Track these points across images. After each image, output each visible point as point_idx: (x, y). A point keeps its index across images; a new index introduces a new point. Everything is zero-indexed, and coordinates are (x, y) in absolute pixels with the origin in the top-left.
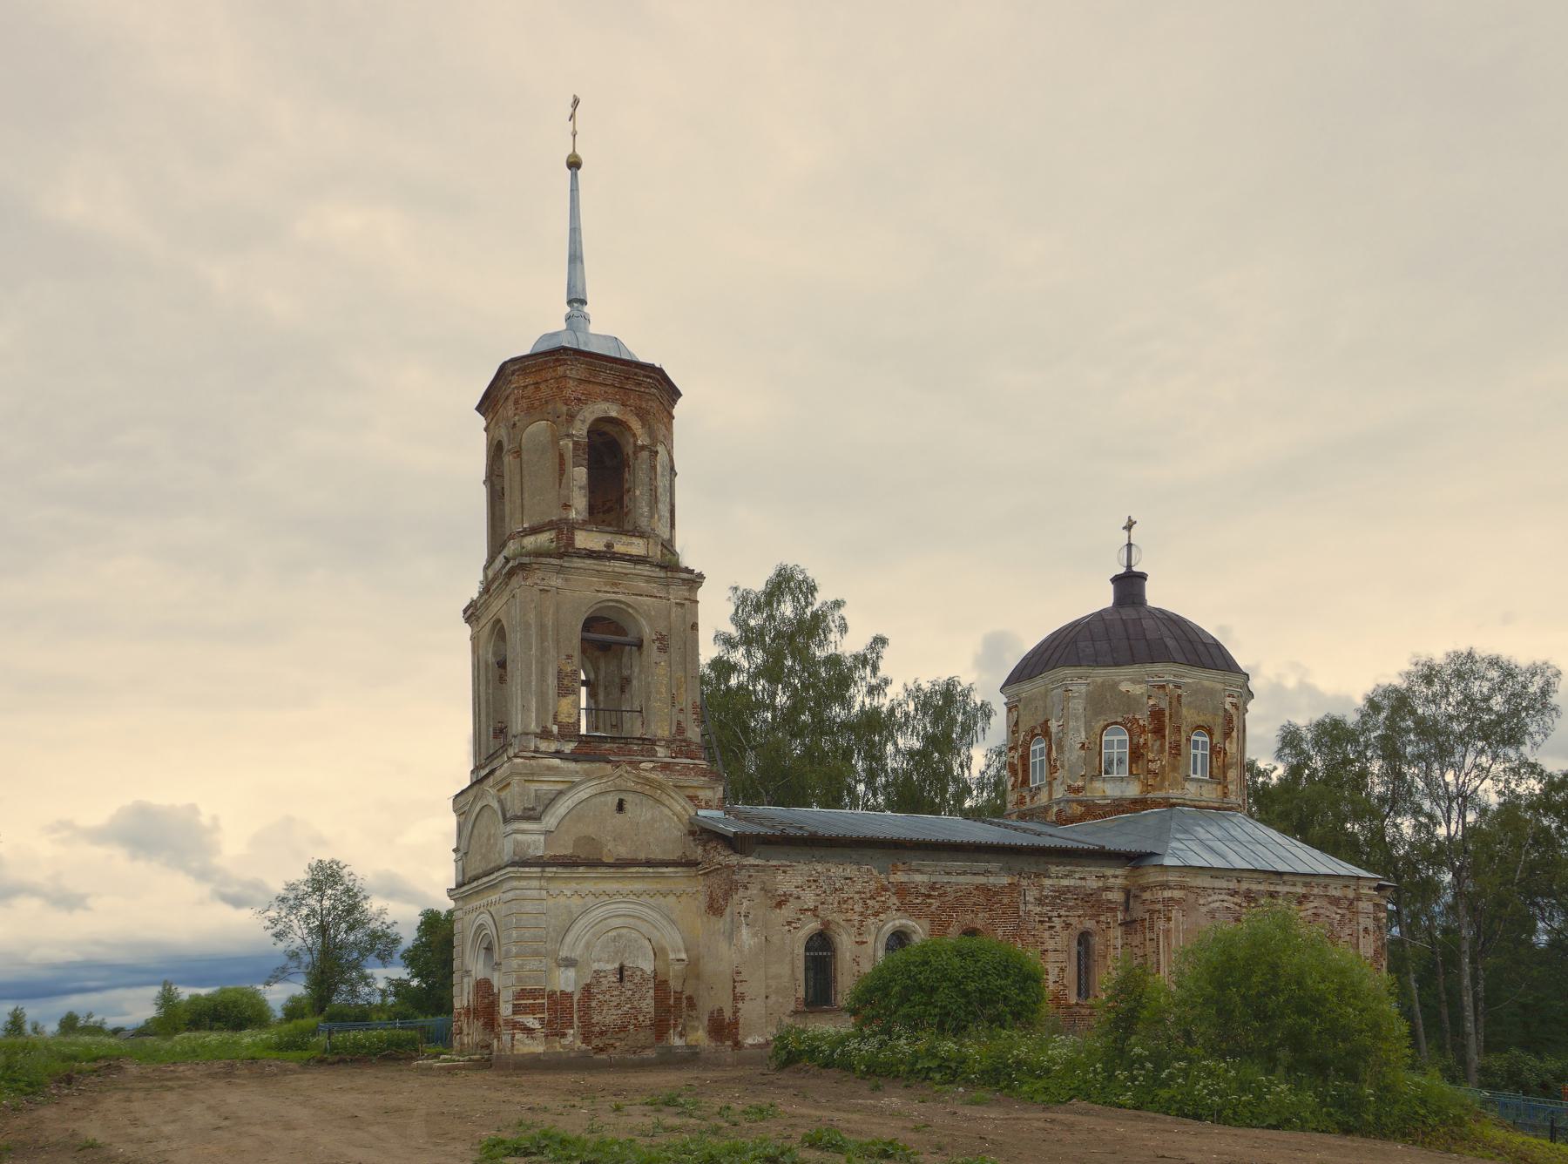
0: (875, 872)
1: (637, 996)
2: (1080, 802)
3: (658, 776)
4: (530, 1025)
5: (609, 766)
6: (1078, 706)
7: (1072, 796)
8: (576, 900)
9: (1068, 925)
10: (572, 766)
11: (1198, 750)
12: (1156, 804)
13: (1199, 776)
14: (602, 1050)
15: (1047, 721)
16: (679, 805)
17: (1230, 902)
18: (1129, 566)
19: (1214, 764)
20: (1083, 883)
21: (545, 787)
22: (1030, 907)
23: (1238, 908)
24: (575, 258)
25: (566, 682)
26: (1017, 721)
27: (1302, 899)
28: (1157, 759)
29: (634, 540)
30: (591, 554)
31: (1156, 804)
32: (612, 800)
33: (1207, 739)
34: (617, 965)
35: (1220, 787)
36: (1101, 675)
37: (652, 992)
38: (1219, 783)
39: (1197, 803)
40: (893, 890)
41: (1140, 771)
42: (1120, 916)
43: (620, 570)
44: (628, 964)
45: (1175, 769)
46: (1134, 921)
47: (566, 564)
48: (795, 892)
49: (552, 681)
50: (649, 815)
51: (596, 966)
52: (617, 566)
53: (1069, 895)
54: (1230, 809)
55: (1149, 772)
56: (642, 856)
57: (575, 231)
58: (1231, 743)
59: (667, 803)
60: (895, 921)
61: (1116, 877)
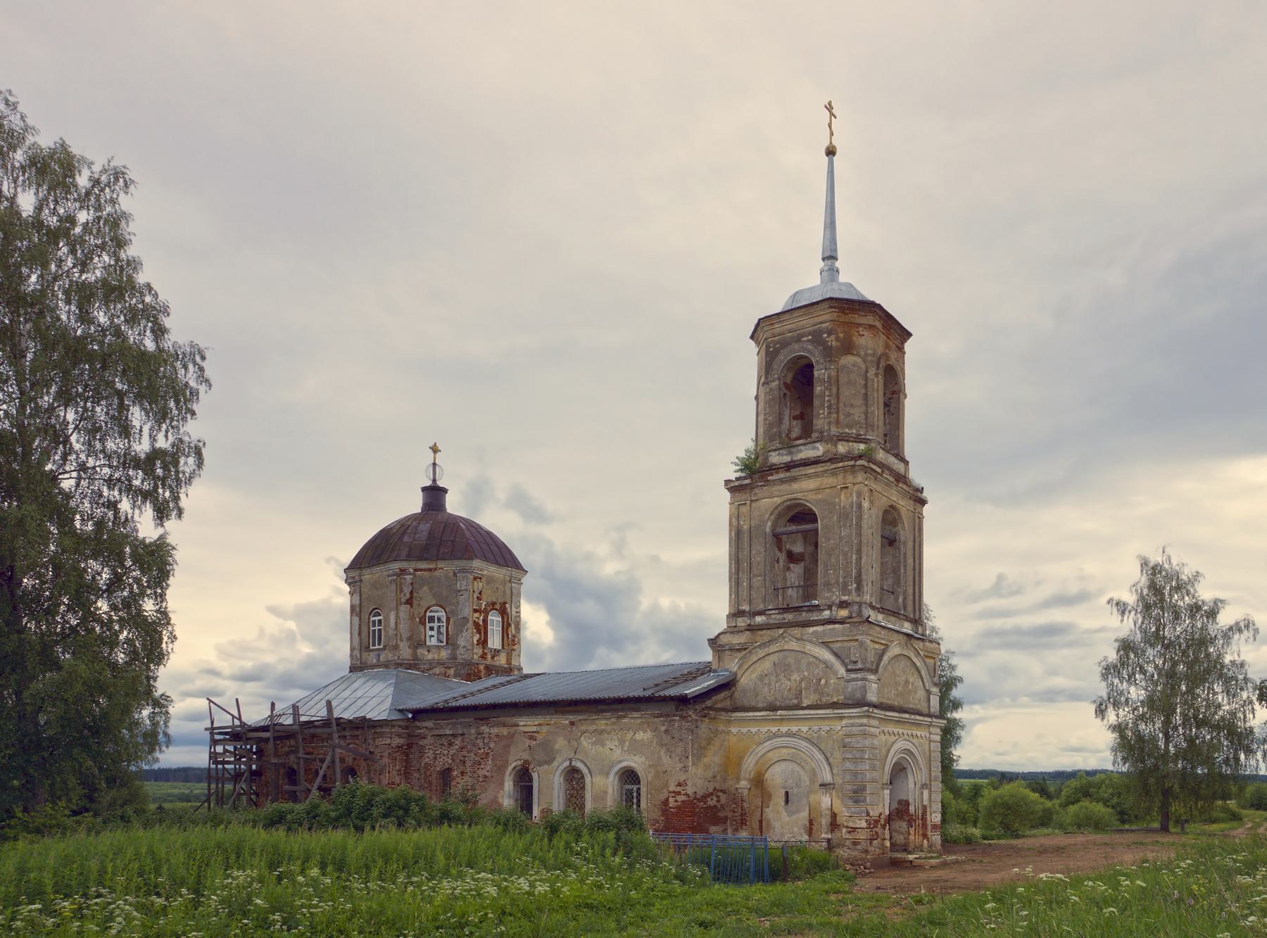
15: (505, 603)
18: (434, 480)
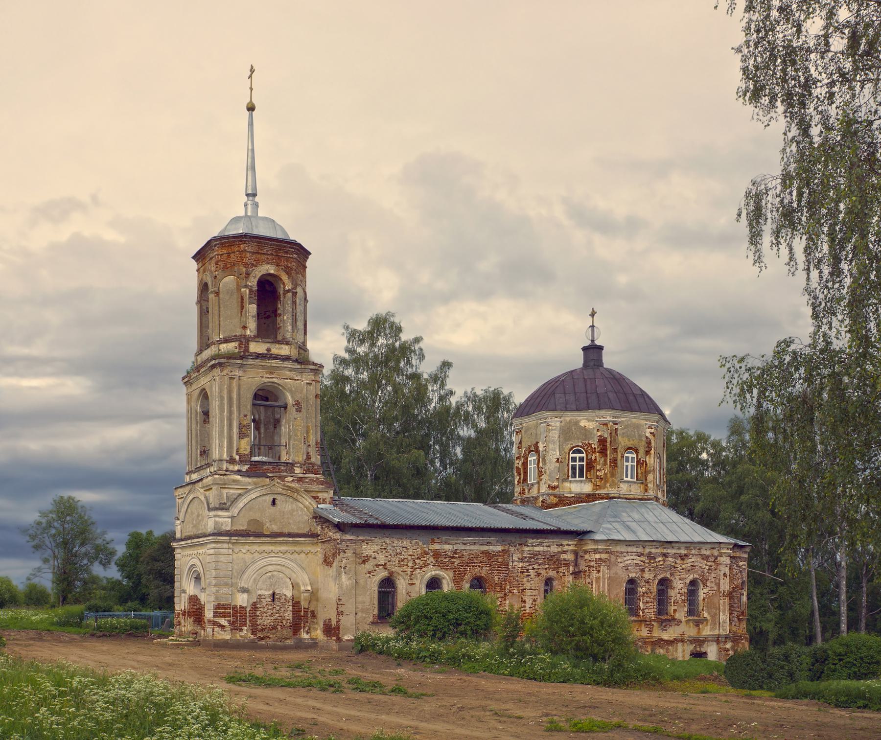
0: (421, 544)
1: (283, 610)
2: (555, 496)
3: (295, 485)
4: (222, 623)
5: (268, 480)
6: (555, 435)
7: (551, 491)
8: (248, 556)
9: (539, 574)
10: (247, 480)
11: (629, 461)
12: (601, 497)
13: (629, 479)
14: (262, 639)
16: (308, 501)
17: (638, 559)
19: (639, 471)
20: (548, 549)
21: (232, 491)
22: (515, 563)
23: (642, 563)
25: (243, 430)
26: (521, 441)
27: (683, 557)
28: (602, 469)
29: (283, 346)
30: (258, 356)
31: (601, 497)
32: (269, 499)
33: (635, 456)
34: (271, 592)
35: (642, 486)
36: (569, 416)
37: (291, 608)
38: (642, 483)
39: (627, 496)
40: (432, 554)
41: (592, 477)
42: (571, 569)
43: (275, 365)
44: (277, 591)
45: (613, 475)
46: (581, 571)
47: (245, 363)
48: (373, 555)
49: (235, 430)
50: (290, 508)
51: (259, 592)
52: (273, 363)
53: (539, 557)
54: (649, 499)
55: (598, 477)
56: (286, 531)
58: (650, 457)
59: (301, 500)
60: (432, 572)
61: (570, 545)
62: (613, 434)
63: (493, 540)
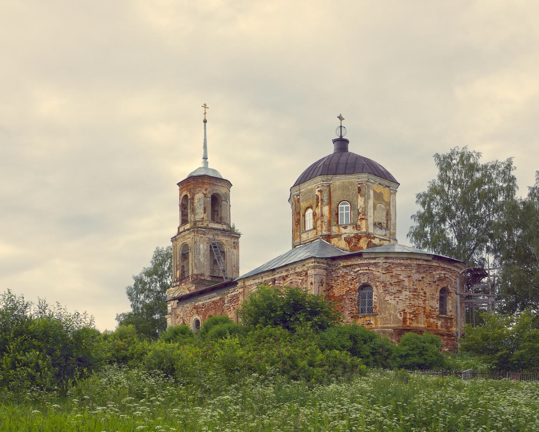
24: (205, 147)
27: (284, 278)
57: (205, 140)
62: (297, 203)
63: (215, 294)
